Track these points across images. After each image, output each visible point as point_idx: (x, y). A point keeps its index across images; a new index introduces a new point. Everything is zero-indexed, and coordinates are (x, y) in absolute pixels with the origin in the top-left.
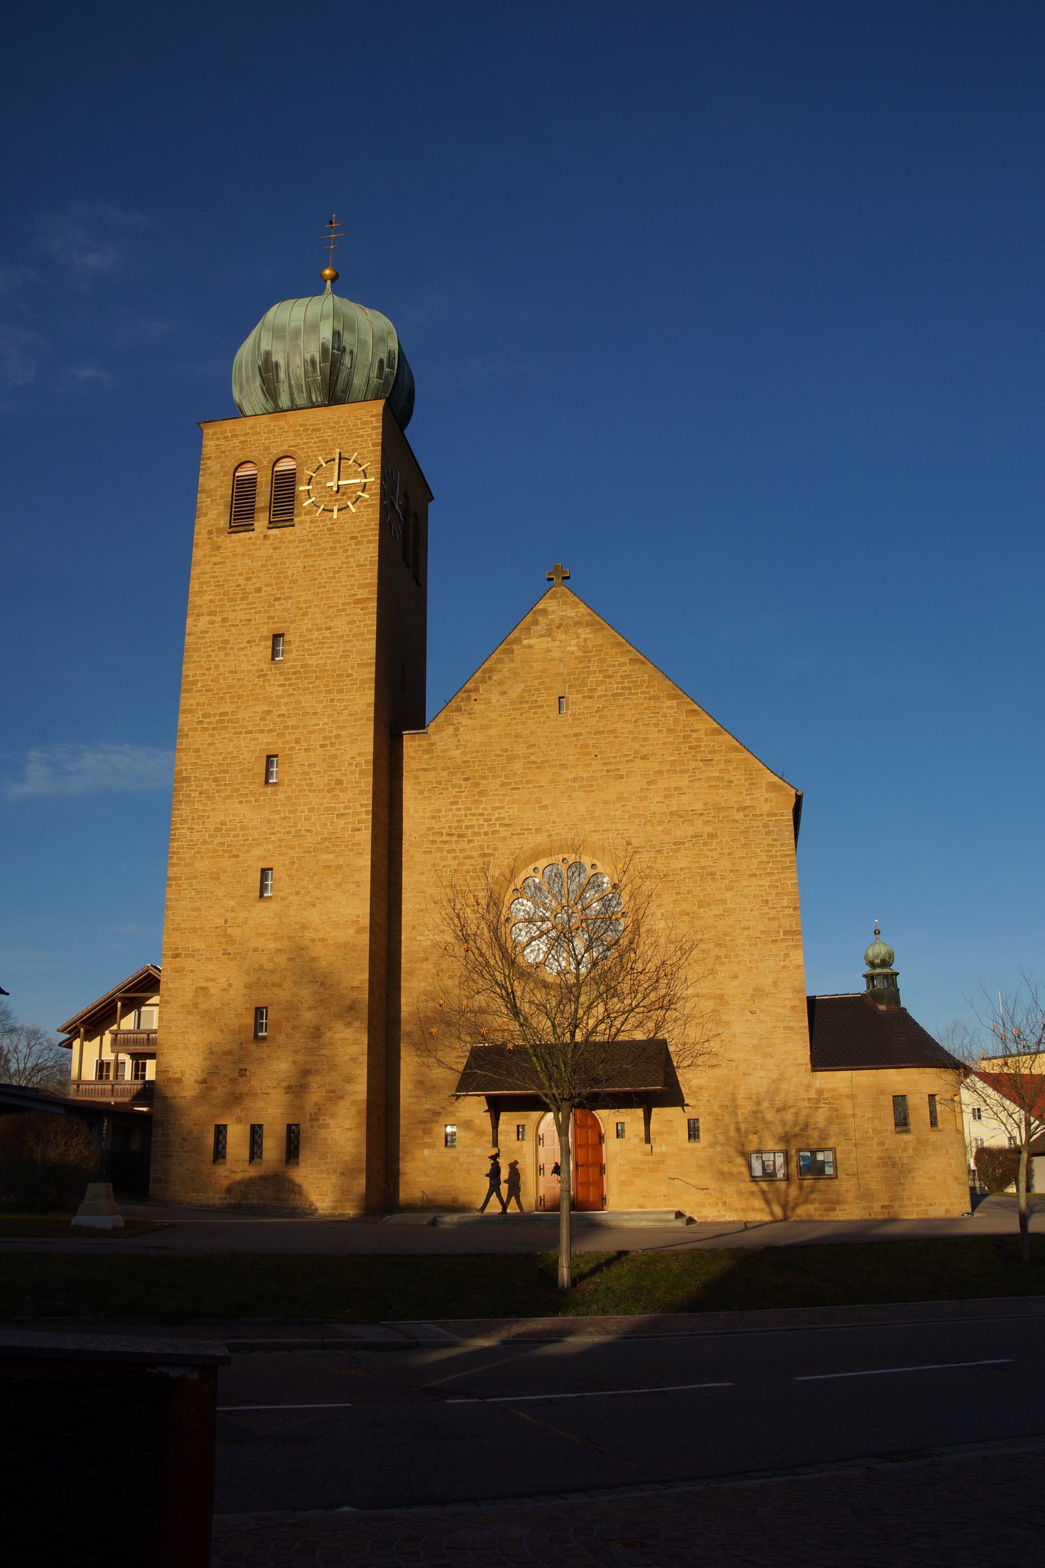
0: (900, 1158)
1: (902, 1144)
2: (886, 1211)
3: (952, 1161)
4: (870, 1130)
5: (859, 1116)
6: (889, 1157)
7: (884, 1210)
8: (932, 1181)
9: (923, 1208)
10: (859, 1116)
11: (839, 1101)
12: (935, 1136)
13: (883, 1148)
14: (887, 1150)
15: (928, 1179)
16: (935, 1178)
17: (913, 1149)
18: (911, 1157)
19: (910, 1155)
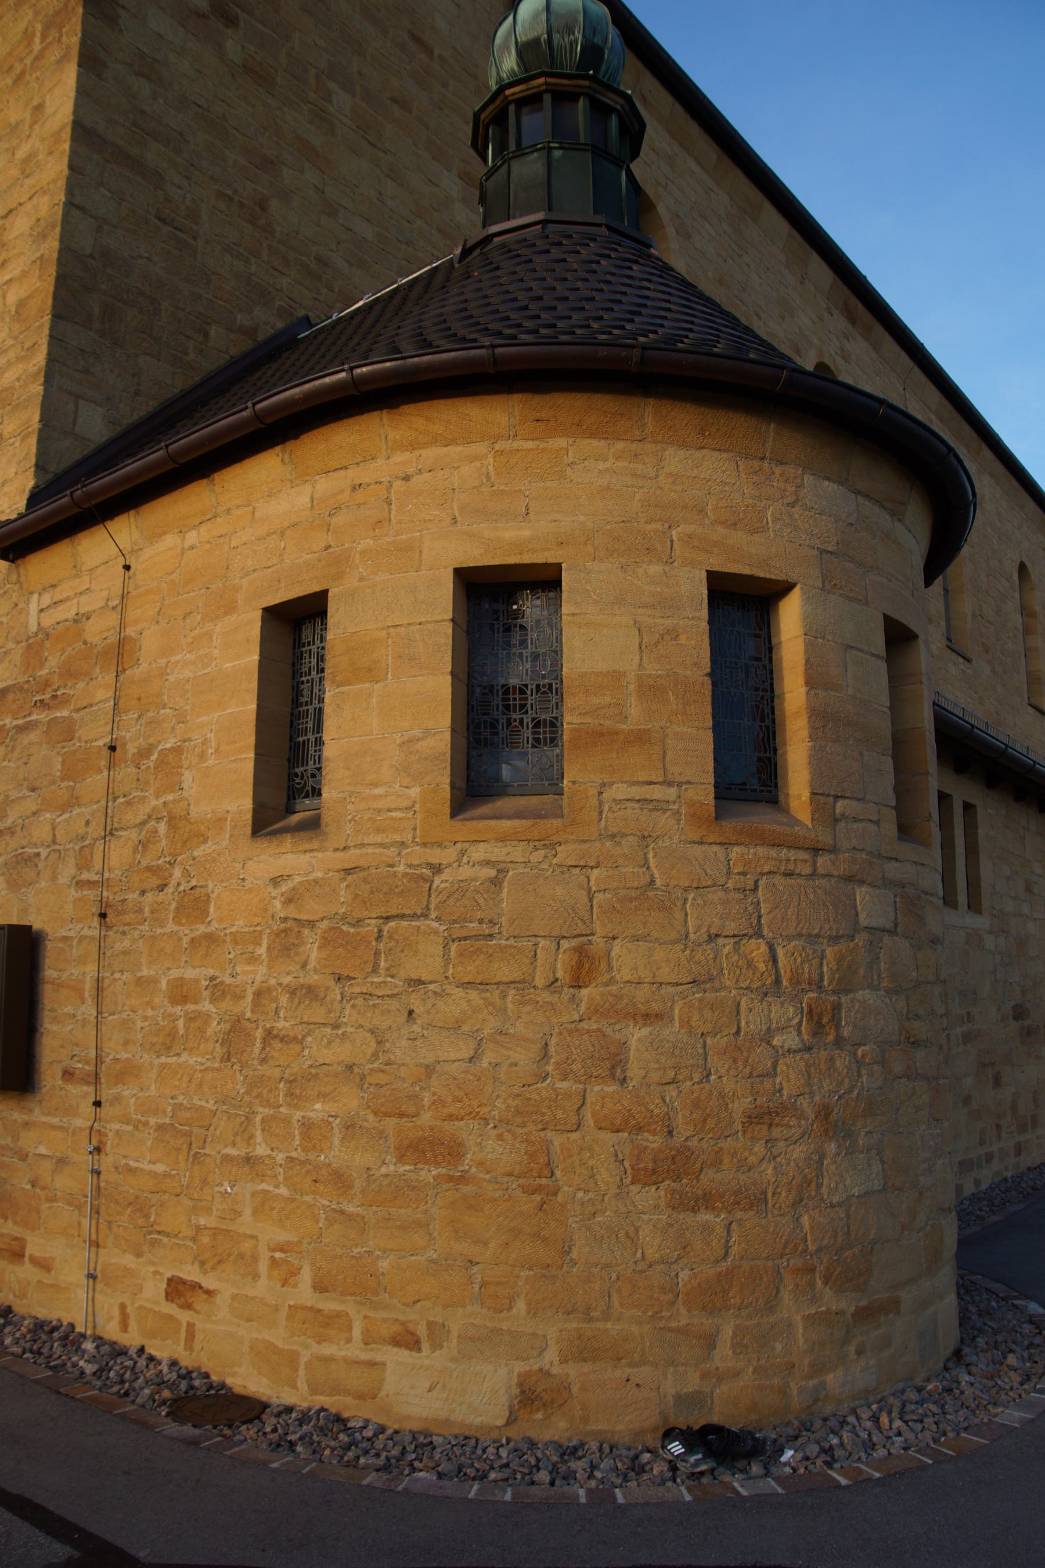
0: (258, 994)
1: (278, 904)
2: (184, 1317)
3: (637, 1035)
4: (162, 828)
5: (132, 749)
6: (218, 990)
7: (171, 1309)
8: (428, 1174)
9: (356, 1351)
10: (132, 749)
11: (81, 685)
12: (478, 852)
13: (202, 929)
14: (211, 939)
15: (401, 1159)
16: (454, 1151)
17: (326, 942)
18: (311, 992)
19: (314, 979)
